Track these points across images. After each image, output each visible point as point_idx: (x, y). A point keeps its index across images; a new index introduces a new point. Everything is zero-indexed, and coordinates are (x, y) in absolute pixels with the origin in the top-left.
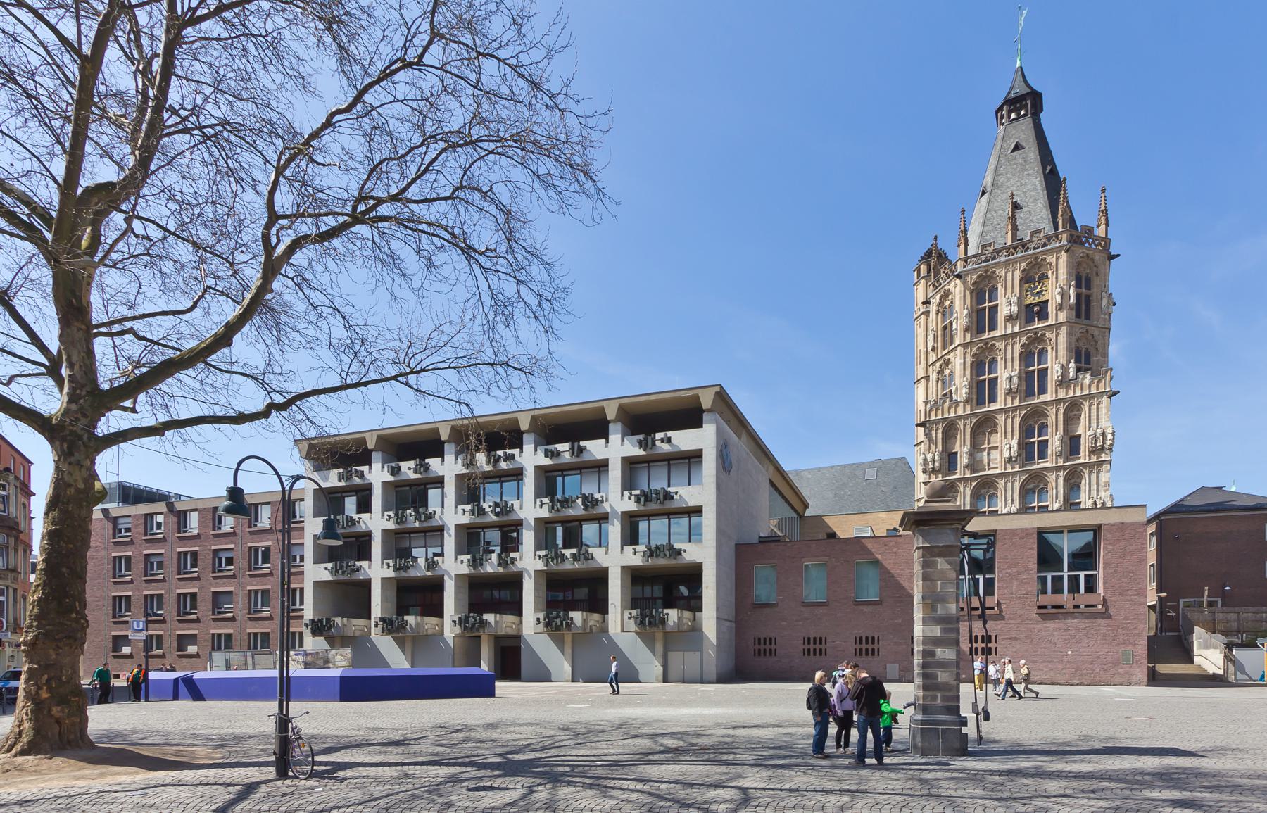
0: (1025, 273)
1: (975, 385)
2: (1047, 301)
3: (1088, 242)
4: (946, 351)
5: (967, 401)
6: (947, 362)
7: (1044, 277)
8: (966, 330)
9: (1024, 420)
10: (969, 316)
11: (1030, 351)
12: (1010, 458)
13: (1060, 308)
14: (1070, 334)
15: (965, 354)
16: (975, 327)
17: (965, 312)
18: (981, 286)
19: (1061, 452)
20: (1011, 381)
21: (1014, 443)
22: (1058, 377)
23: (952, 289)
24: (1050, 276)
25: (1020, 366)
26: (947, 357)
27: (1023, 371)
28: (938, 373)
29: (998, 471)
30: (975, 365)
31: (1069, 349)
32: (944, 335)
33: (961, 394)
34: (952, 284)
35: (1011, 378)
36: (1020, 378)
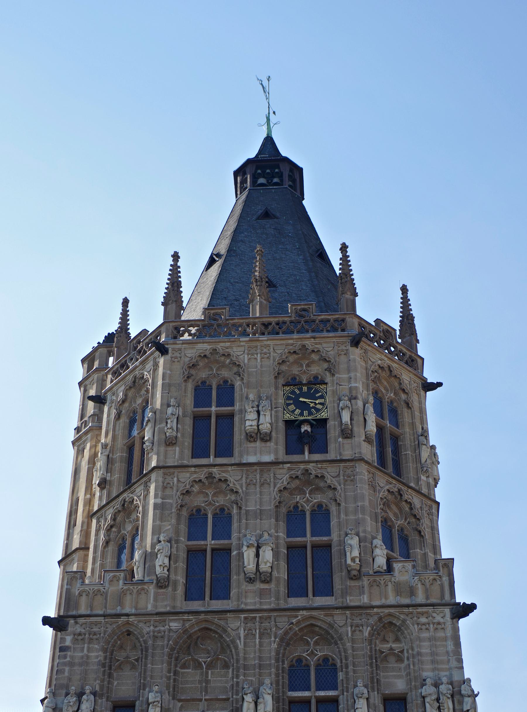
11: (296, 507)
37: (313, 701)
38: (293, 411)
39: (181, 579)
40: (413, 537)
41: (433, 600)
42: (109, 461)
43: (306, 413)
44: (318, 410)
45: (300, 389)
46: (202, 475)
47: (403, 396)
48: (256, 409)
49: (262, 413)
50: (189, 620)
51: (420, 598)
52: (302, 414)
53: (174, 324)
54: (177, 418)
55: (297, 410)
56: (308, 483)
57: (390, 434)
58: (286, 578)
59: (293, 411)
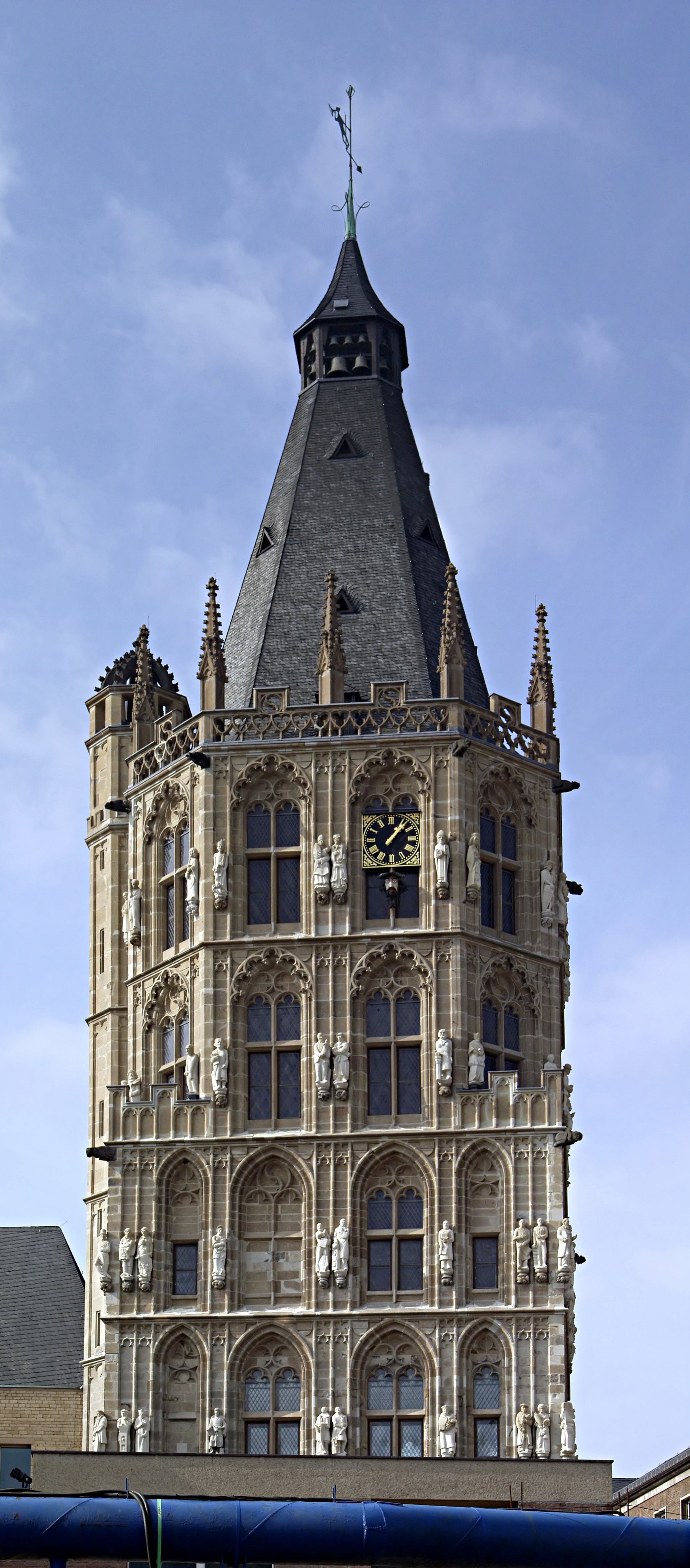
0: (363, 786)
1: (242, 1061)
2: (416, 870)
3: (508, 737)
4: (168, 954)
5: (224, 1102)
6: (170, 986)
7: (406, 806)
8: (222, 907)
9: (365, 1173)
10: (229, 871)
11: (378, 992)
12: (330, 1275)
13: (445, 893)
14: (469, 965)
15: (217, 971)
16: (241, 900)
17: (218, 859)
18: (259, 797)
19: (452, 1276)
20: (331, 1066)
21: (341, 1234)
22: (444, 1072)
23: (185, 790)
24: (421, 806)
25: (353, 1029)
26: (172, 971)
27: (360, 1044)
28: (150, 1010)
29: (299, 1310)
30: (242, 1005)
31: (467, 1005)
32: (165, 906)
33: (208, 1080)
34: (186, 775)
35: (331, 1058)
36: (353, 1062)
37: (394, 1242)
38: (376, 855)
39: (242, 1093)
40: (525, 1018)
42: (142, 908)
43: (392, 857)
44: (407, 853)
47: (524, 808)
48: (327, 858)
49: (335, 865)
52: (386, 860)
53: (216, 716)
54: (227, 870)
55: (381, 853)
57: (503, 869)
58: (366, 1090)
59: (376, 855)
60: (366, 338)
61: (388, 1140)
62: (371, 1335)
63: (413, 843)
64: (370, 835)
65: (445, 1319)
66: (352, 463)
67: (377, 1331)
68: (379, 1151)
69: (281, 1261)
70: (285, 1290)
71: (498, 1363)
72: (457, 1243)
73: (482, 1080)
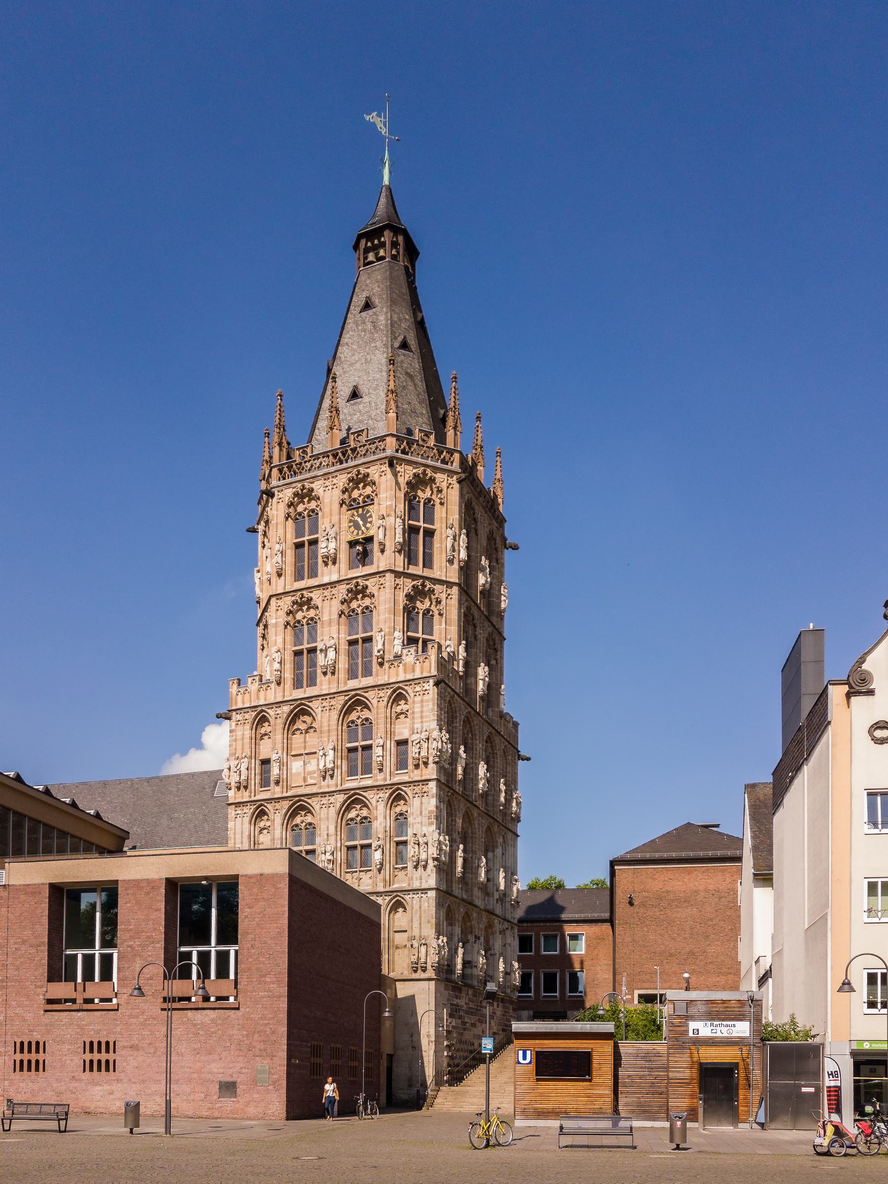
39: (288, 675)
41: (425, 675)
45: (357, 512)
46: (297, 597)
50: (293, 705)
51: (417, 675)
56: (357, 592)
59: (353, 532)
60: (393, 238)
61: (354, 693)
62: (345, 801)
63: (371, 523)
64: (350, 521)
65: (379, 787)
66: (370, 312)
67: (349, 798)
68: (350, 699)
69: (308, 765)
70: (310, 781)
71: (407, 812)
72: (385, 747)
73: (399, 653)
